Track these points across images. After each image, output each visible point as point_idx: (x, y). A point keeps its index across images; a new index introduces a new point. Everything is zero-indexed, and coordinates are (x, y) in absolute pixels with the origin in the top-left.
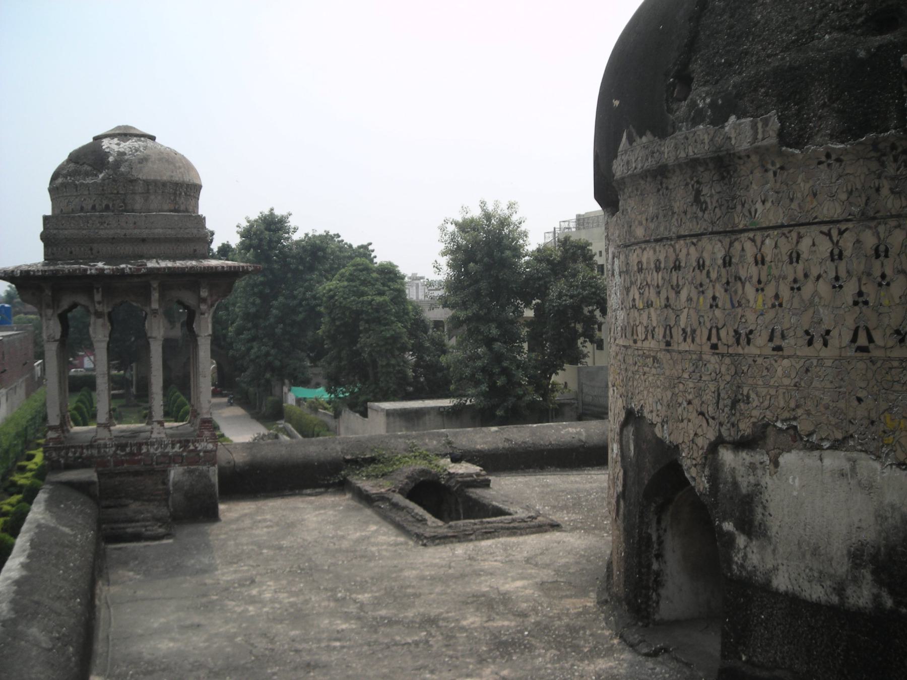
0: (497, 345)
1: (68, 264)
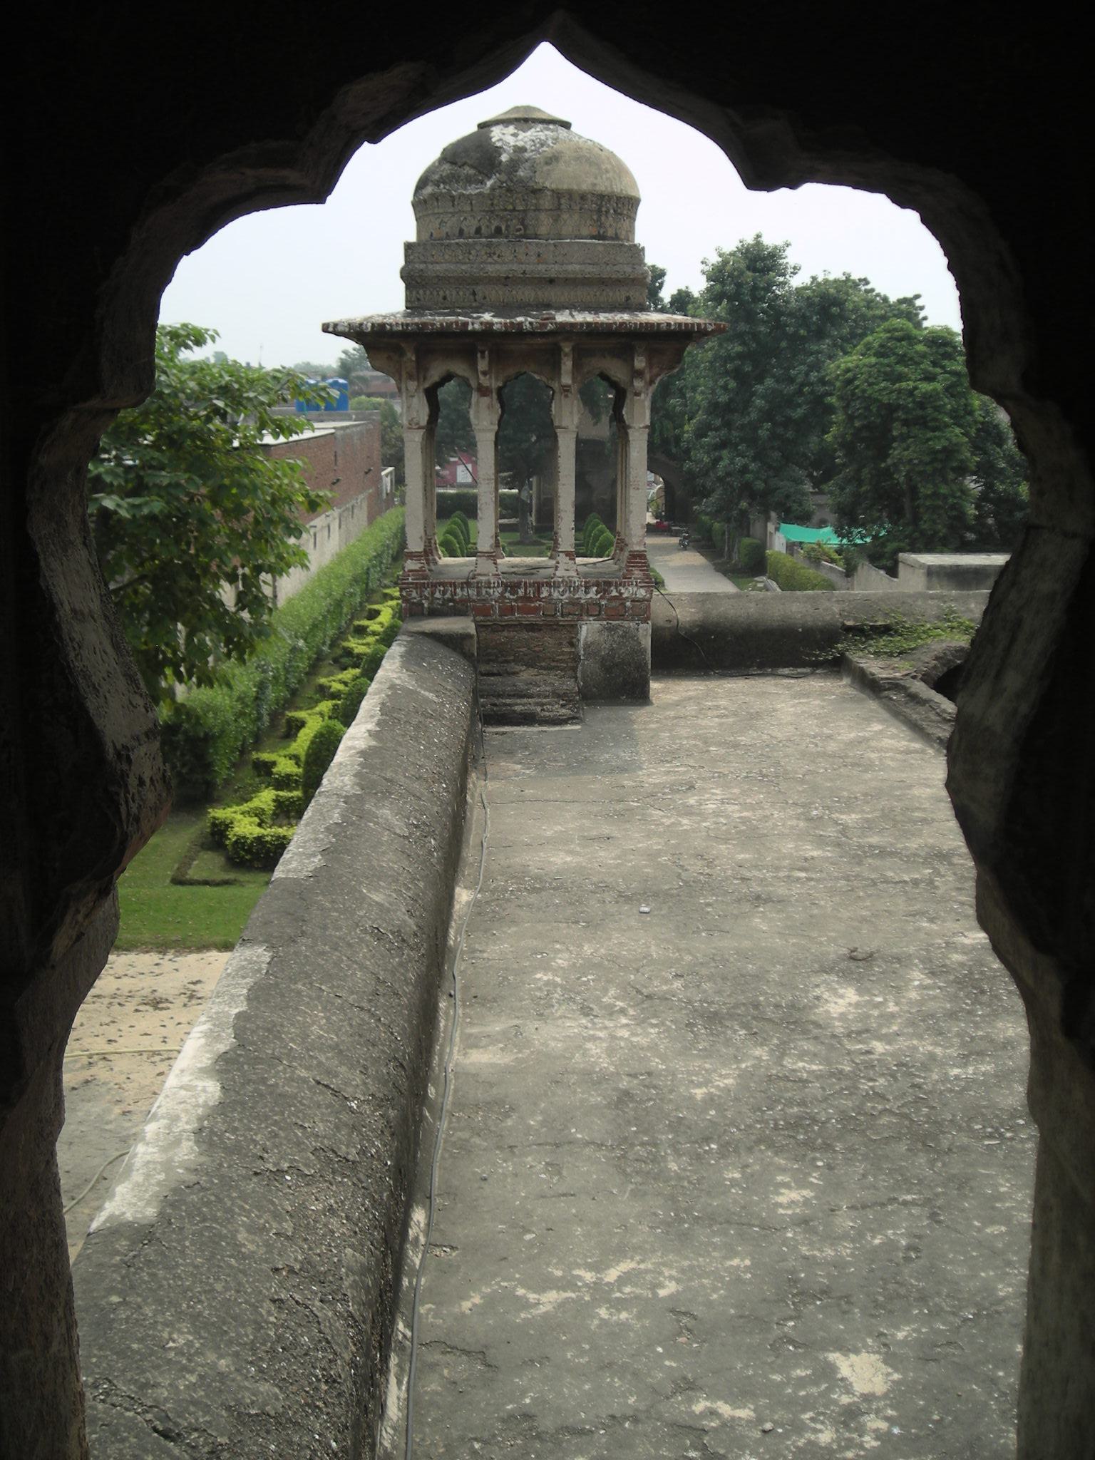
1: (440, 314)
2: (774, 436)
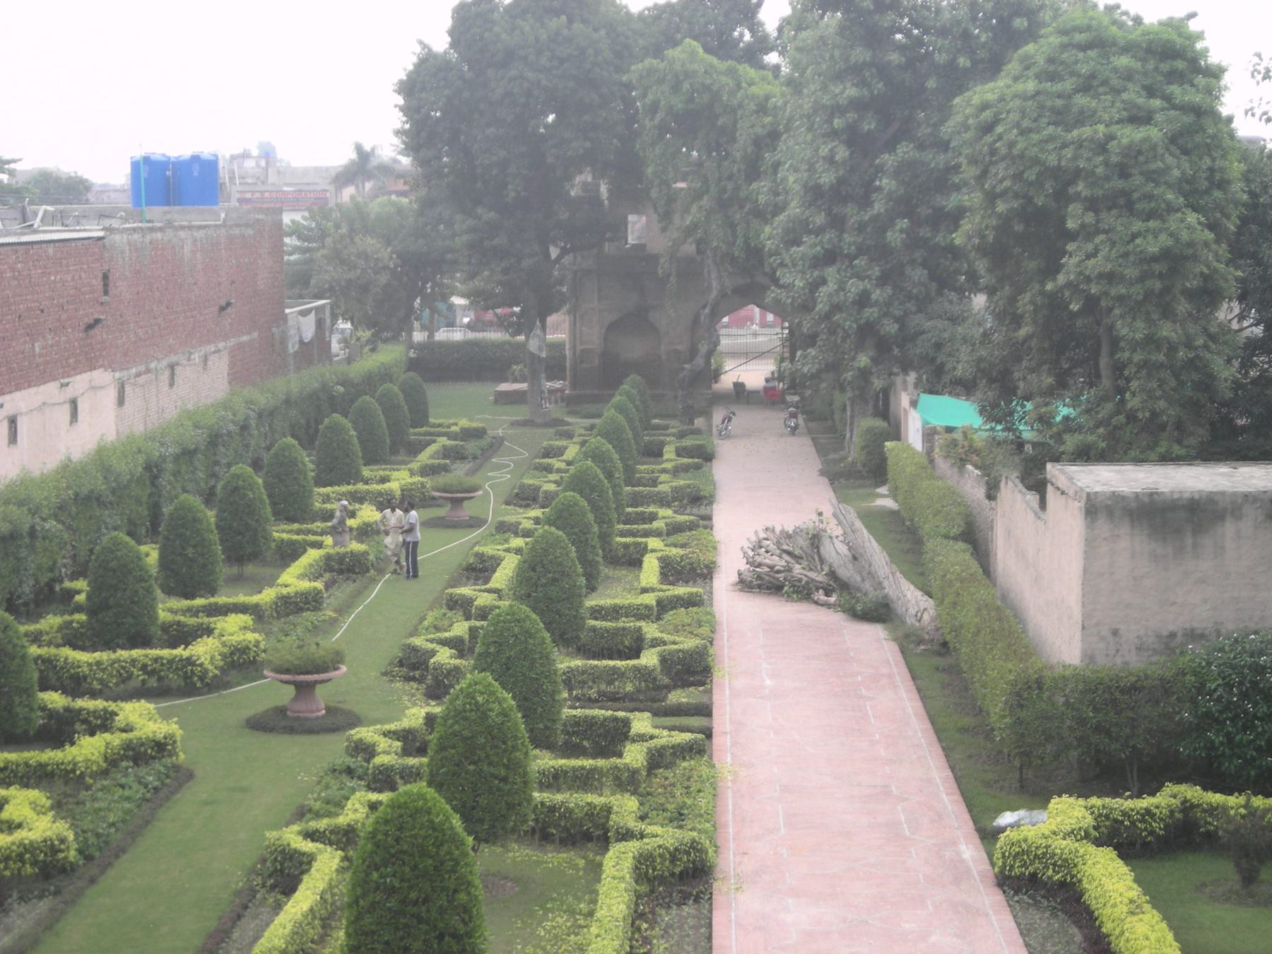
2: (913, 242)
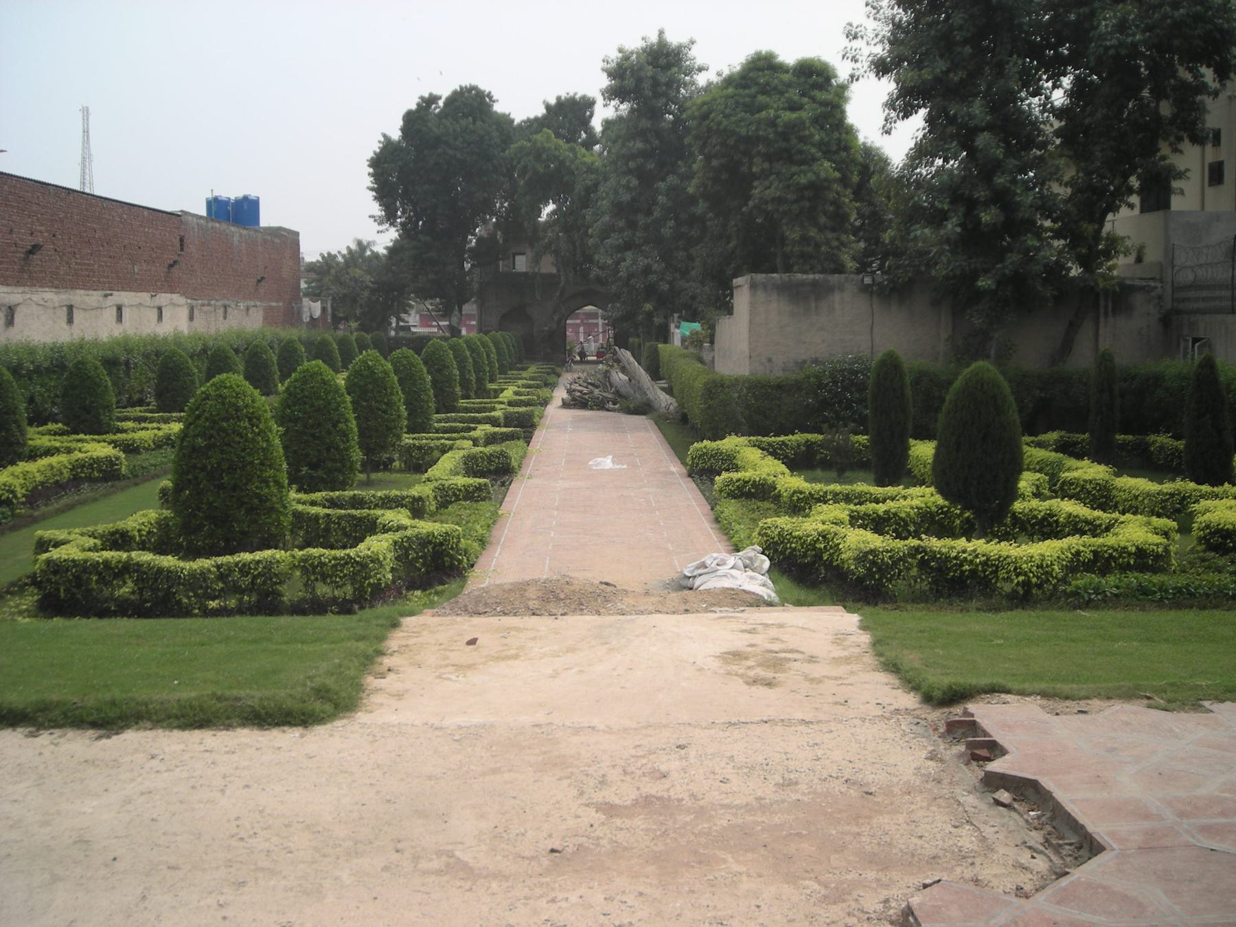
0: (983, 139)
